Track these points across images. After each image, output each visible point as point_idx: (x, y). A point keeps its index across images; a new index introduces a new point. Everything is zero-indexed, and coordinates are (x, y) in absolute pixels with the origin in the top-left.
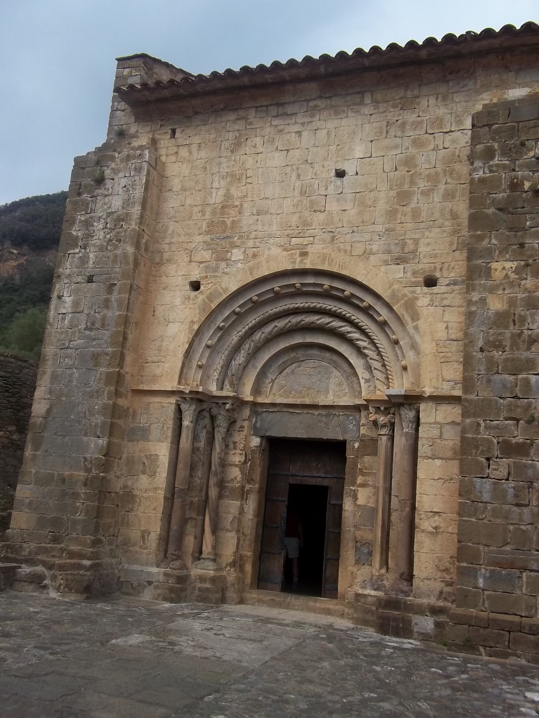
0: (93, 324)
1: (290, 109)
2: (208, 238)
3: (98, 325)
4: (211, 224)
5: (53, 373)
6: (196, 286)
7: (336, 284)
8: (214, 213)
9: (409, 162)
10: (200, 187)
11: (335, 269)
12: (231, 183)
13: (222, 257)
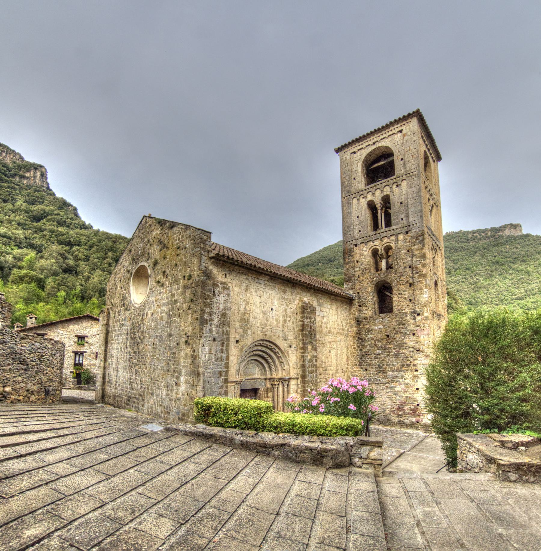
0: (218, 359)
1: (261, 282)
2: (240, 324)
3: (220, 359)
4: (241, 319)
5: (204, 380)
6: (237, 342)
7: (271, 345)
8: (242, 314)
9: (285, 310)
10: (236, 302)
11: (273, 341)
12: (246, 304)
13: (245, 332)
